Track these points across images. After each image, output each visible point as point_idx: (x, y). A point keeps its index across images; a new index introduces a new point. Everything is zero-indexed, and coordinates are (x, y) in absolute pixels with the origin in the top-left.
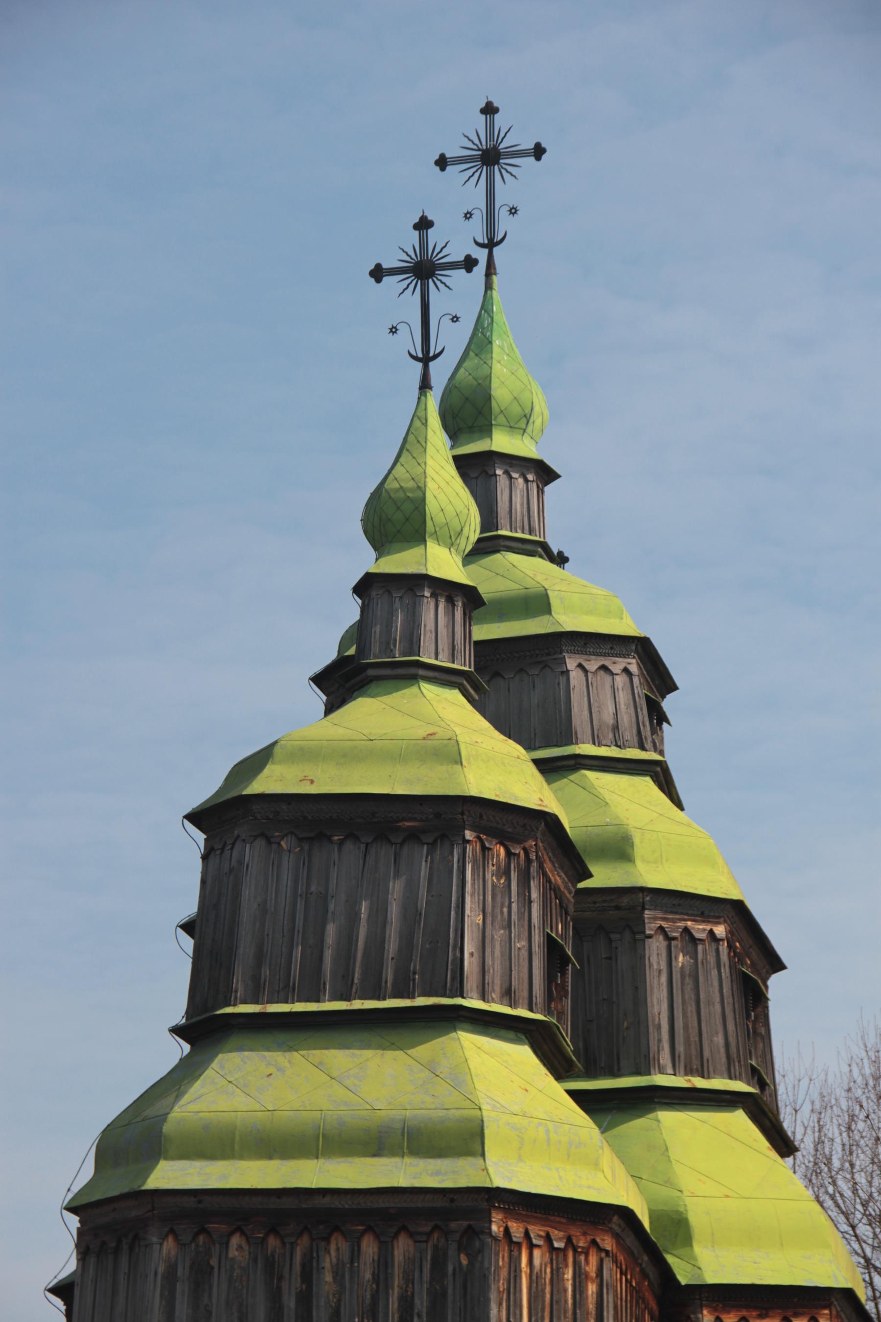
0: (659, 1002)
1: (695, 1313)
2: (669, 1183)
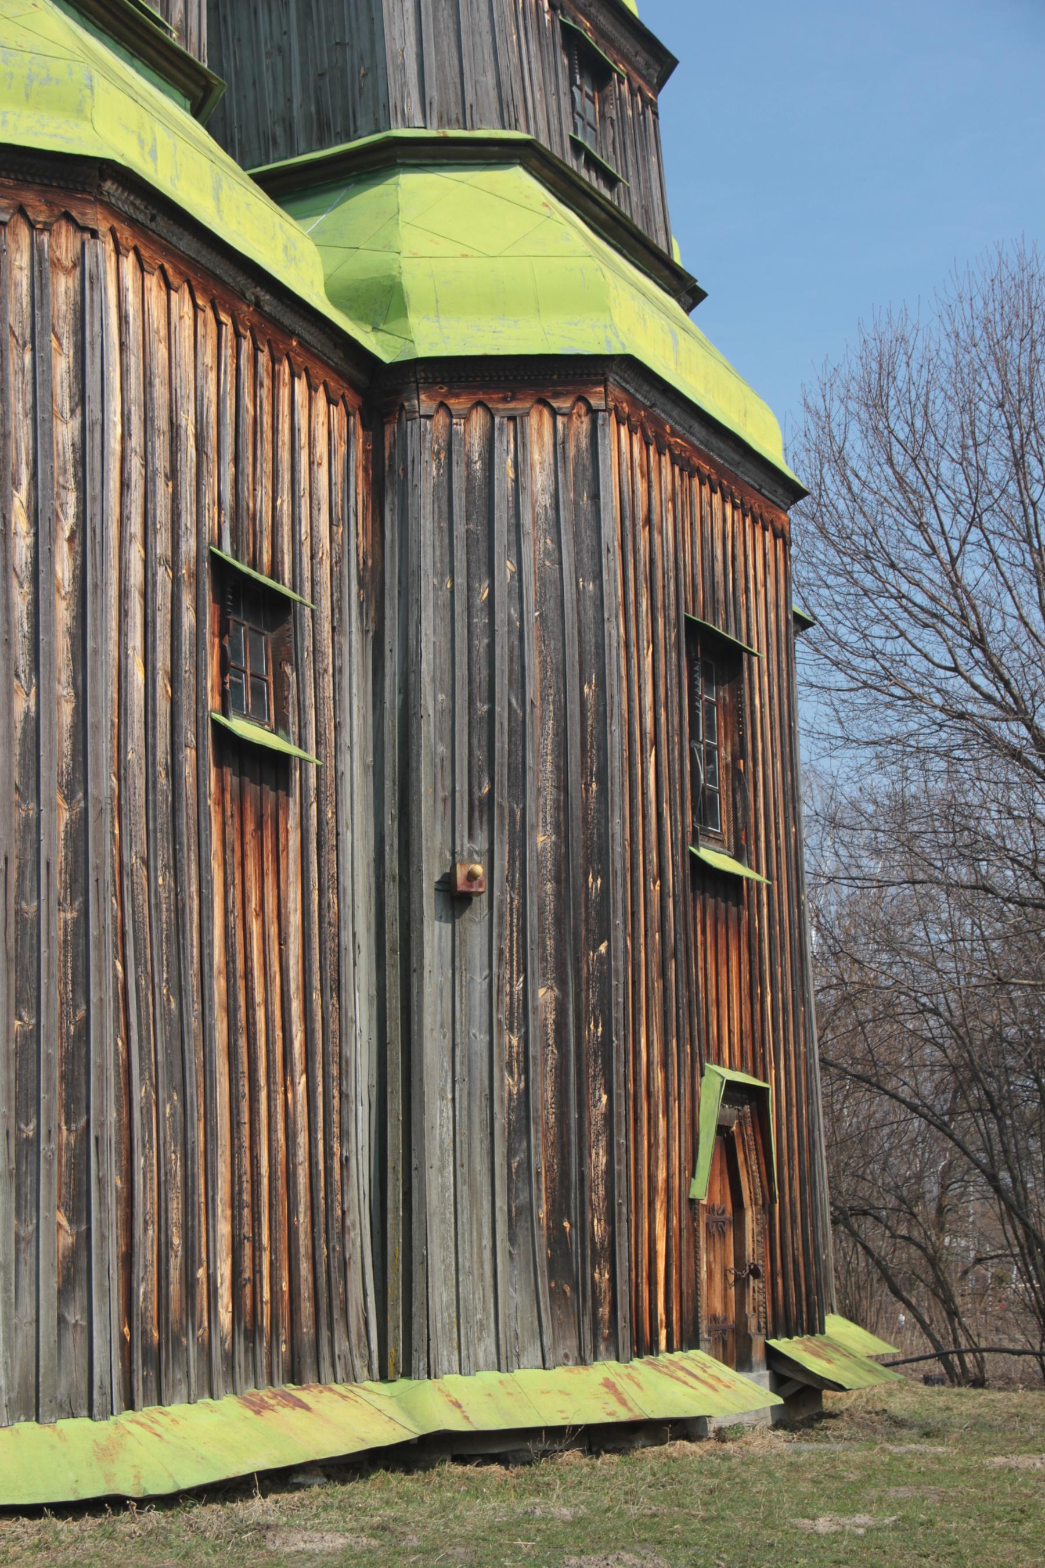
0: (403, 34)
1: (409, 400)
2: (388, 247)
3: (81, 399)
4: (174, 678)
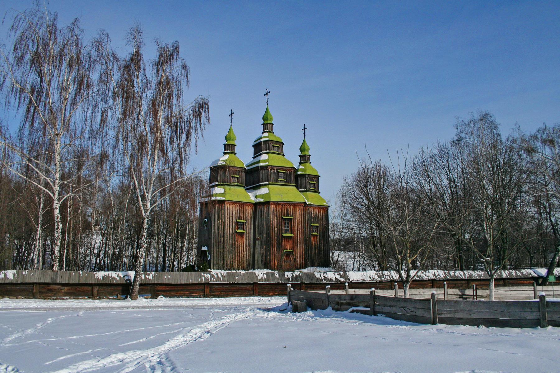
3: (224, 214)
4: (232, 229)
